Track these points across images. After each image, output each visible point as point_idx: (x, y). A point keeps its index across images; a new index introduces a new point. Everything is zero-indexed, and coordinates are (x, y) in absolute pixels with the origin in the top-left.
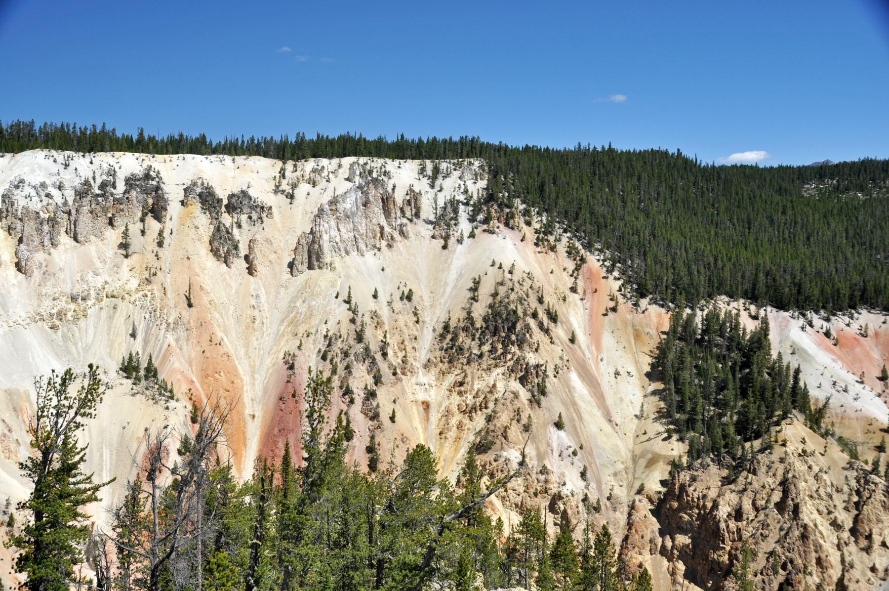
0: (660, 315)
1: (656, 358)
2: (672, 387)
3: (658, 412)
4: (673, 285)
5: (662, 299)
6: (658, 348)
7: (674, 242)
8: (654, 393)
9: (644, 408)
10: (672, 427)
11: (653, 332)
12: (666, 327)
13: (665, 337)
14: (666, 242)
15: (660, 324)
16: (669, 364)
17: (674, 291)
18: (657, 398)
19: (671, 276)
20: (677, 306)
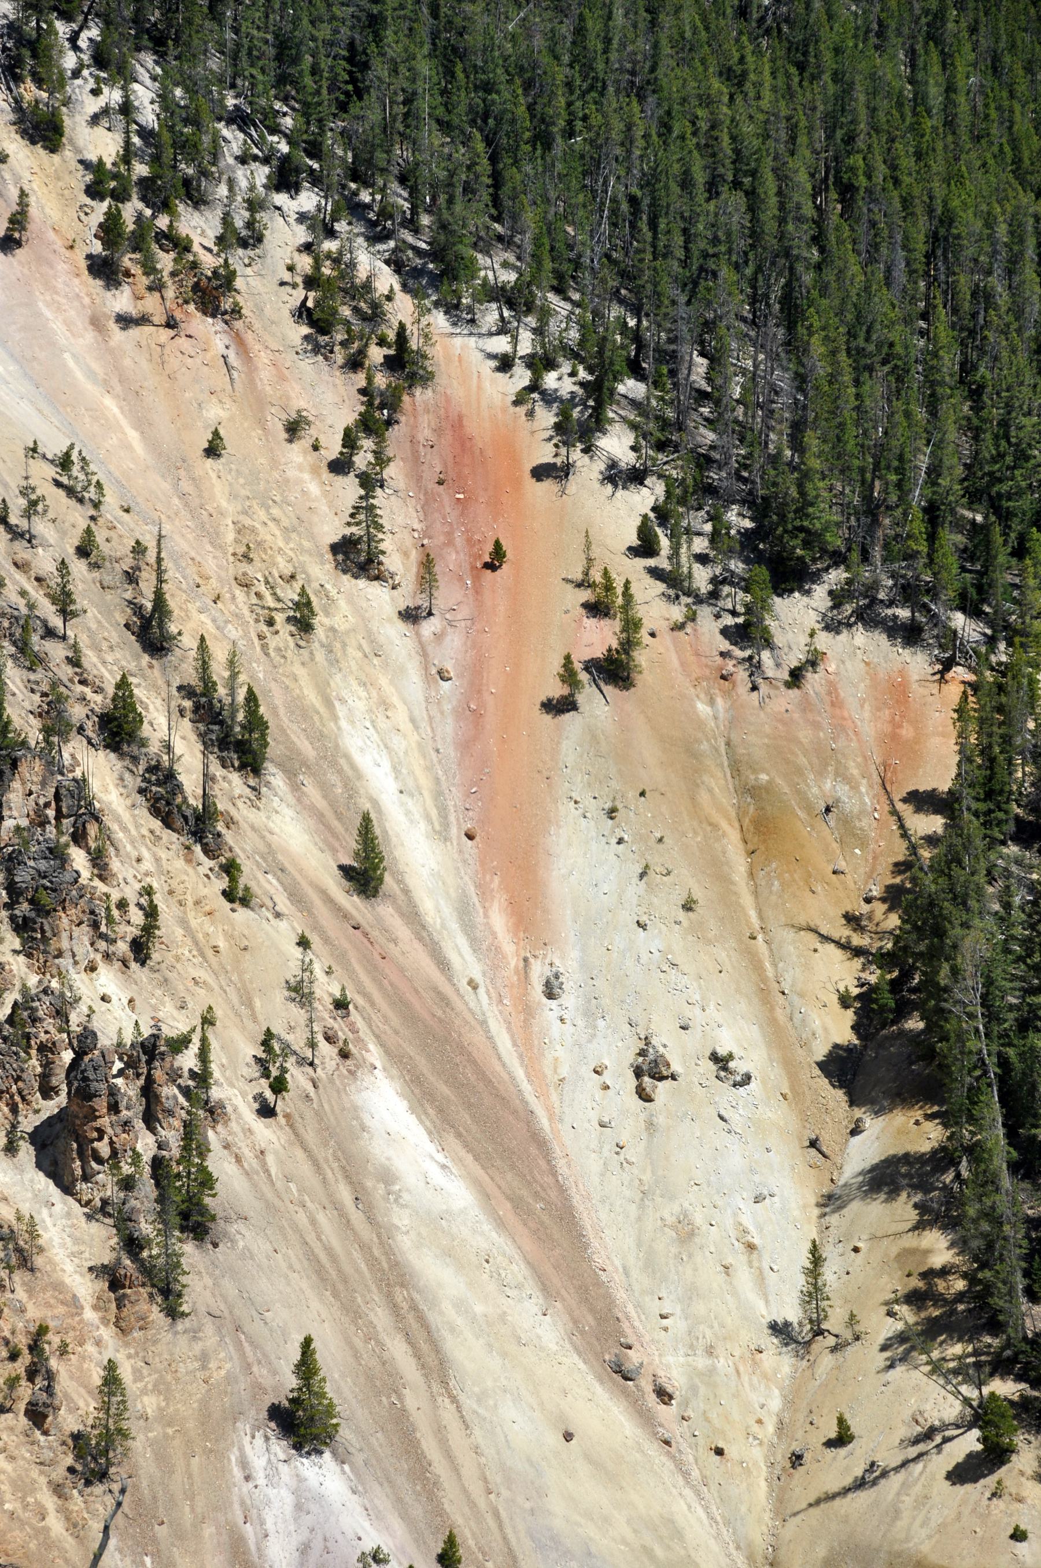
0: (896, 694)
1: (885, 960)
2: (995, 1136)
3: (915, 1299)
4: (973, 497)
5: (908, 593)
6: (893, 897)
7: (969, 223)
8: (883, 1179)
9: (829, 1274)
10: (1005, 1388)
11: (862, 799)
12: (940, 772)
13: (934, 824)
14: (920, 230)
15: (898, 747)
16: (967, 995)
17: (977, 548)
18: (903, 1209)
19: (957, 445)
20: (1002, 630)
